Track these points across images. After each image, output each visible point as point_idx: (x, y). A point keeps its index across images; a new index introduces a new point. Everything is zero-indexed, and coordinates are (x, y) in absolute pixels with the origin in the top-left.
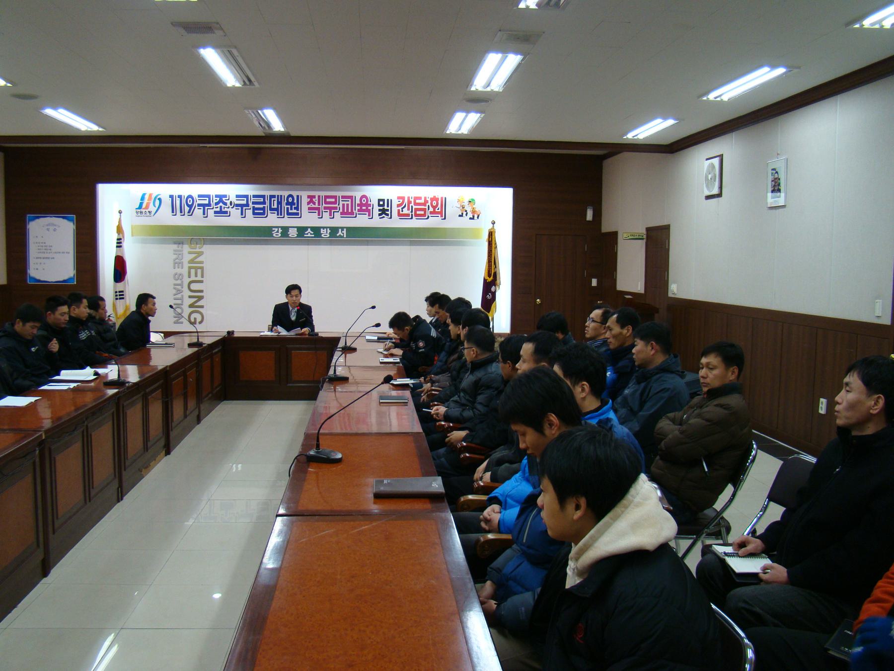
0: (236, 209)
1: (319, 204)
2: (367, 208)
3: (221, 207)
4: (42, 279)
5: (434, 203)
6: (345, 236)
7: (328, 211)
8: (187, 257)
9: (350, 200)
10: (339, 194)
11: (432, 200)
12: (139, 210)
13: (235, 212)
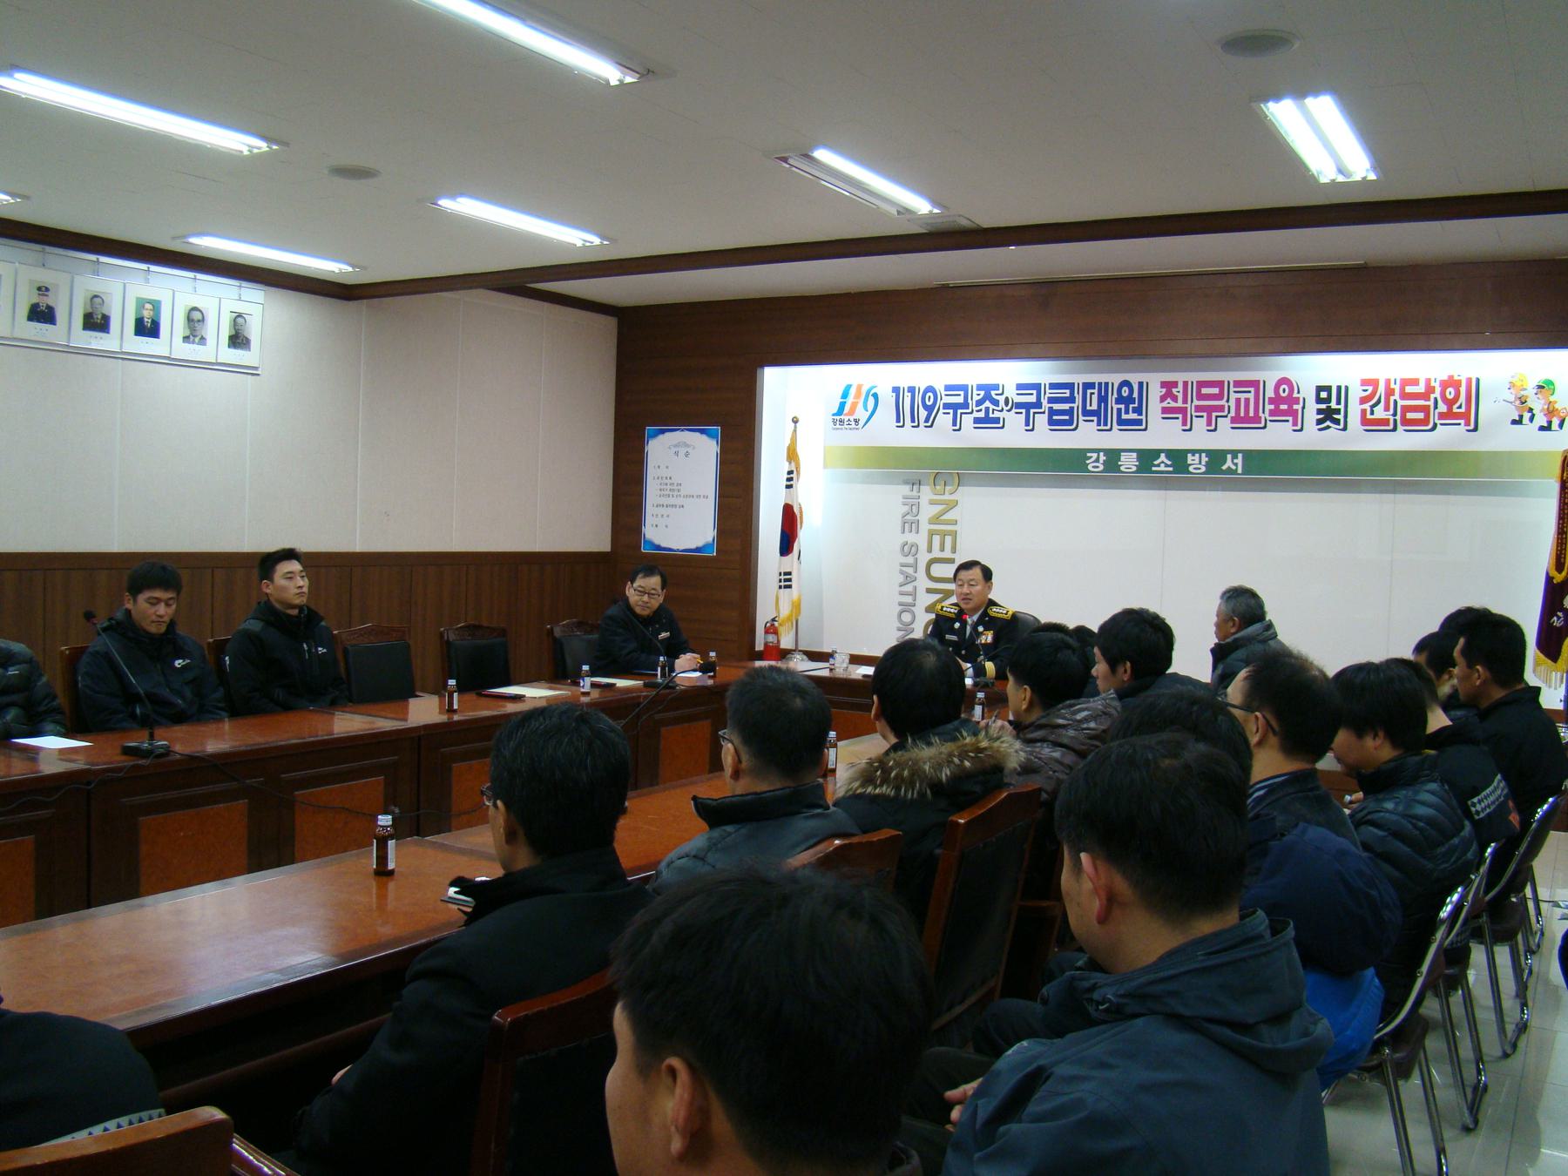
0: (1017, 413)
1: (1185, 401)
2: (1290, 407)
3: (987, 409)
4: (664, 545)
6: (1240, 471)
7: (1205, 414)
8: (927, 512)
9: (1252, 389)
10: (1229, 376)
11: (1445, 385)
12: (838, 418)
13: (1015, 420)
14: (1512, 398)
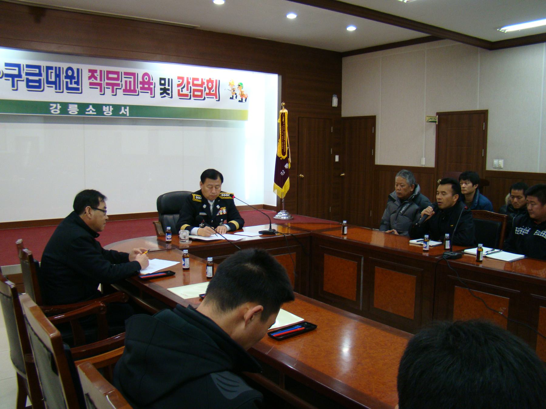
1: (101, 80)
5: (210, 86)
6: (128, 115)
7: (111, 87)
9: (132, 77)
10: (122, 70)
14: (231, 89)
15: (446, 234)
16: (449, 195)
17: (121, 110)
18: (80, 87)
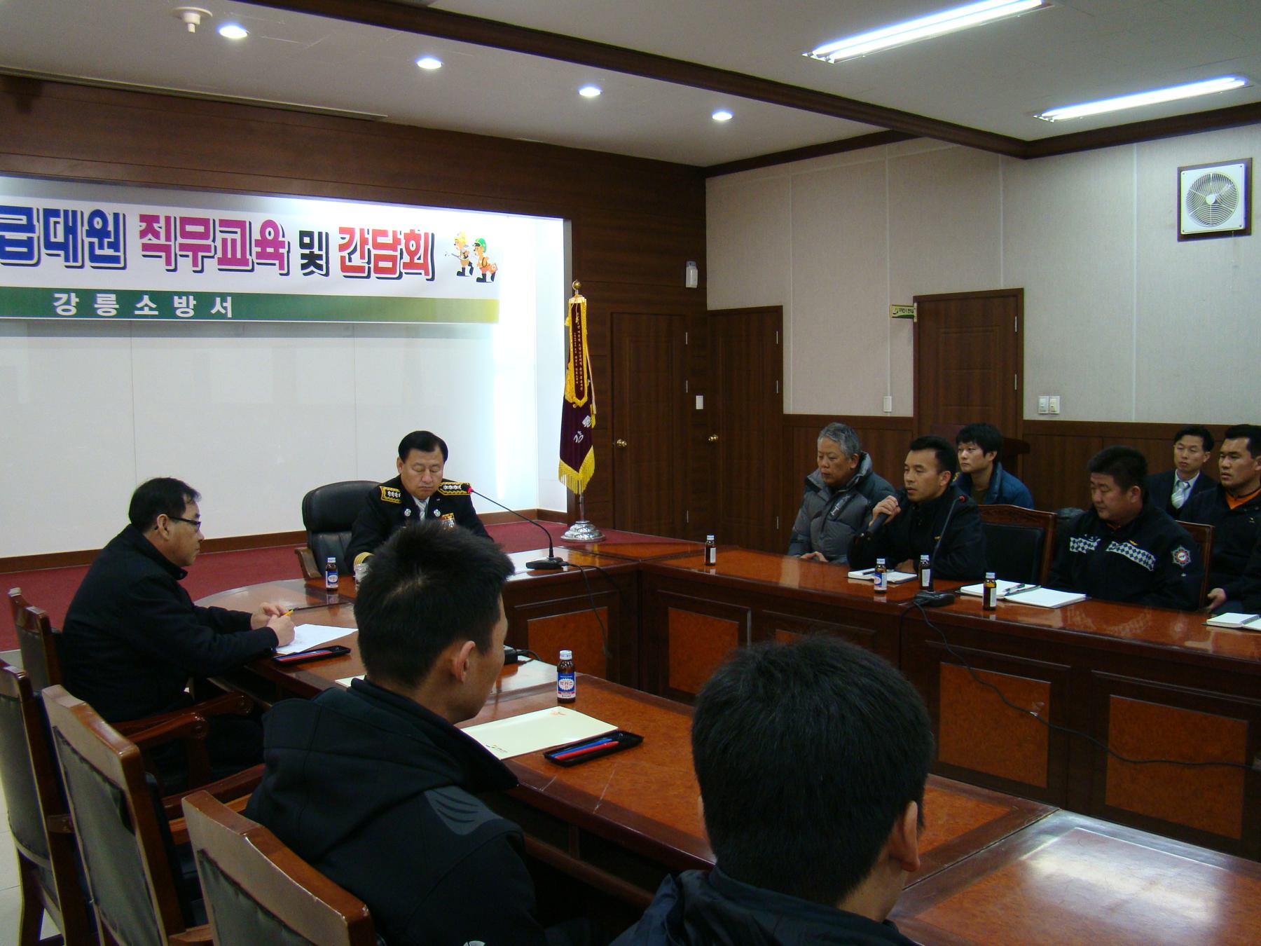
1: (168, 238)
6: (230, 315)
7: (190, 254)
9: (239, 230)
10: (214, 215)
15: (922, 556)
16: (930, 473)
17: (213, 305)
18: (121, 254)
